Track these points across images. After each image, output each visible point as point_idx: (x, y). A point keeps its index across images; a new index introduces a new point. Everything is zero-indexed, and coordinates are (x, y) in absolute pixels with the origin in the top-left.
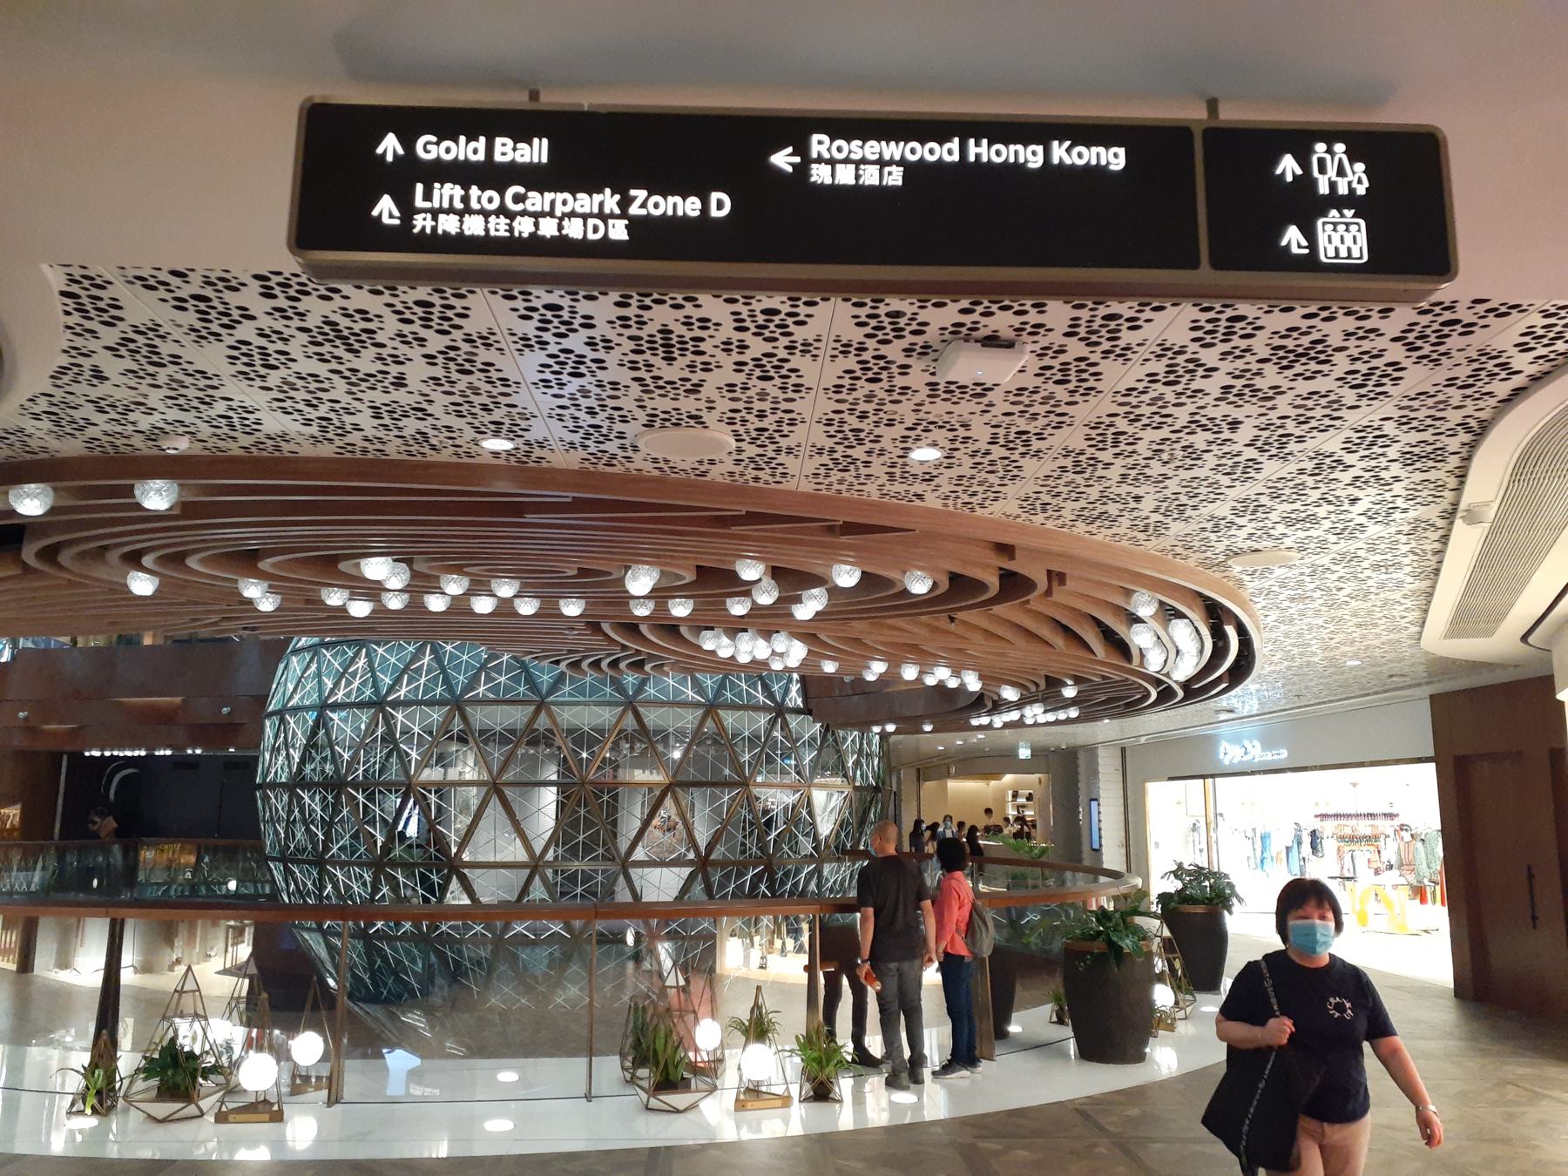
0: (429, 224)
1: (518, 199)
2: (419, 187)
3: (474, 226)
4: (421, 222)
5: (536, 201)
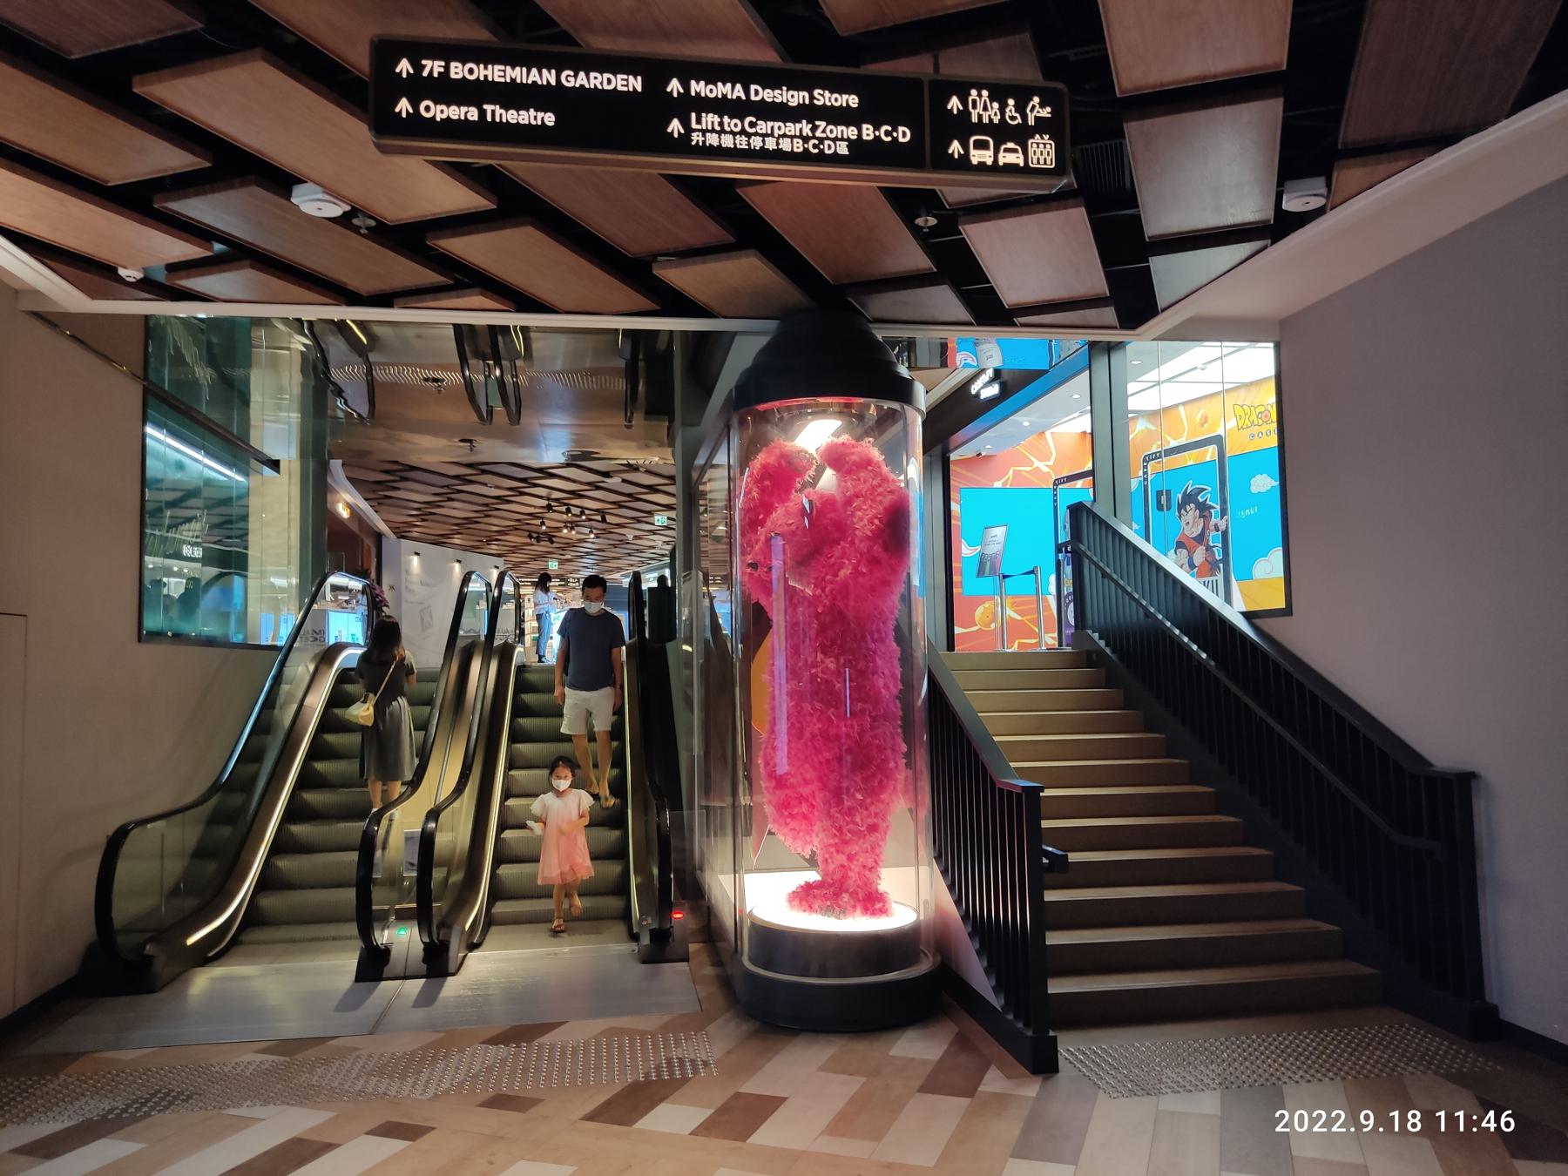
0: (701, 139)
1: (752, 125)
2: (693, 115)
3: (727, 141)
4: (696, 138)
5: (763, 127)
